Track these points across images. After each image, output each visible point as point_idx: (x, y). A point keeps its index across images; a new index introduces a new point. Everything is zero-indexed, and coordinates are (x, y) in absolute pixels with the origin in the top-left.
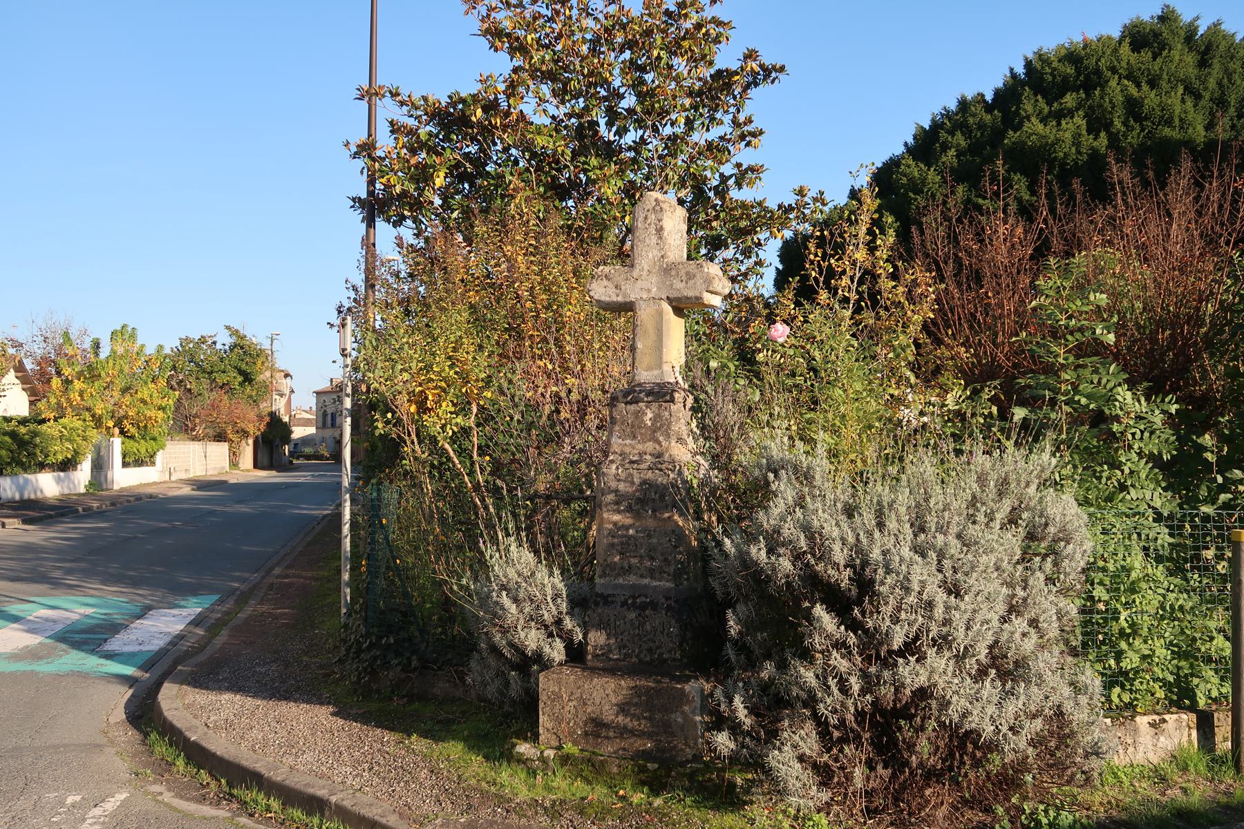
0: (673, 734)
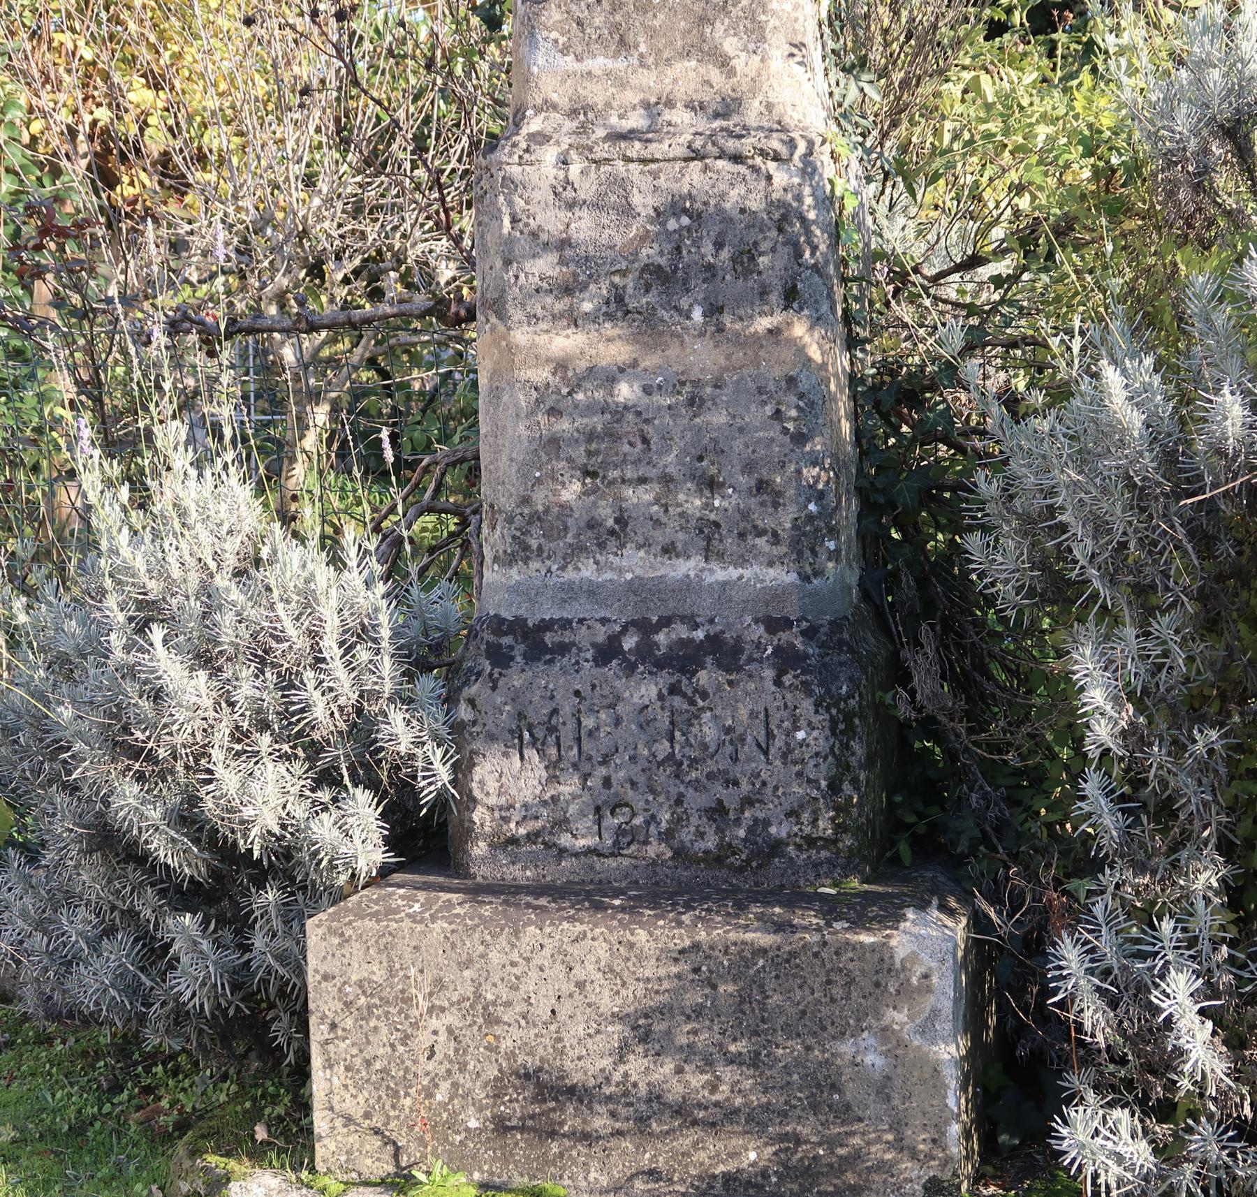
0: (845, 1113)
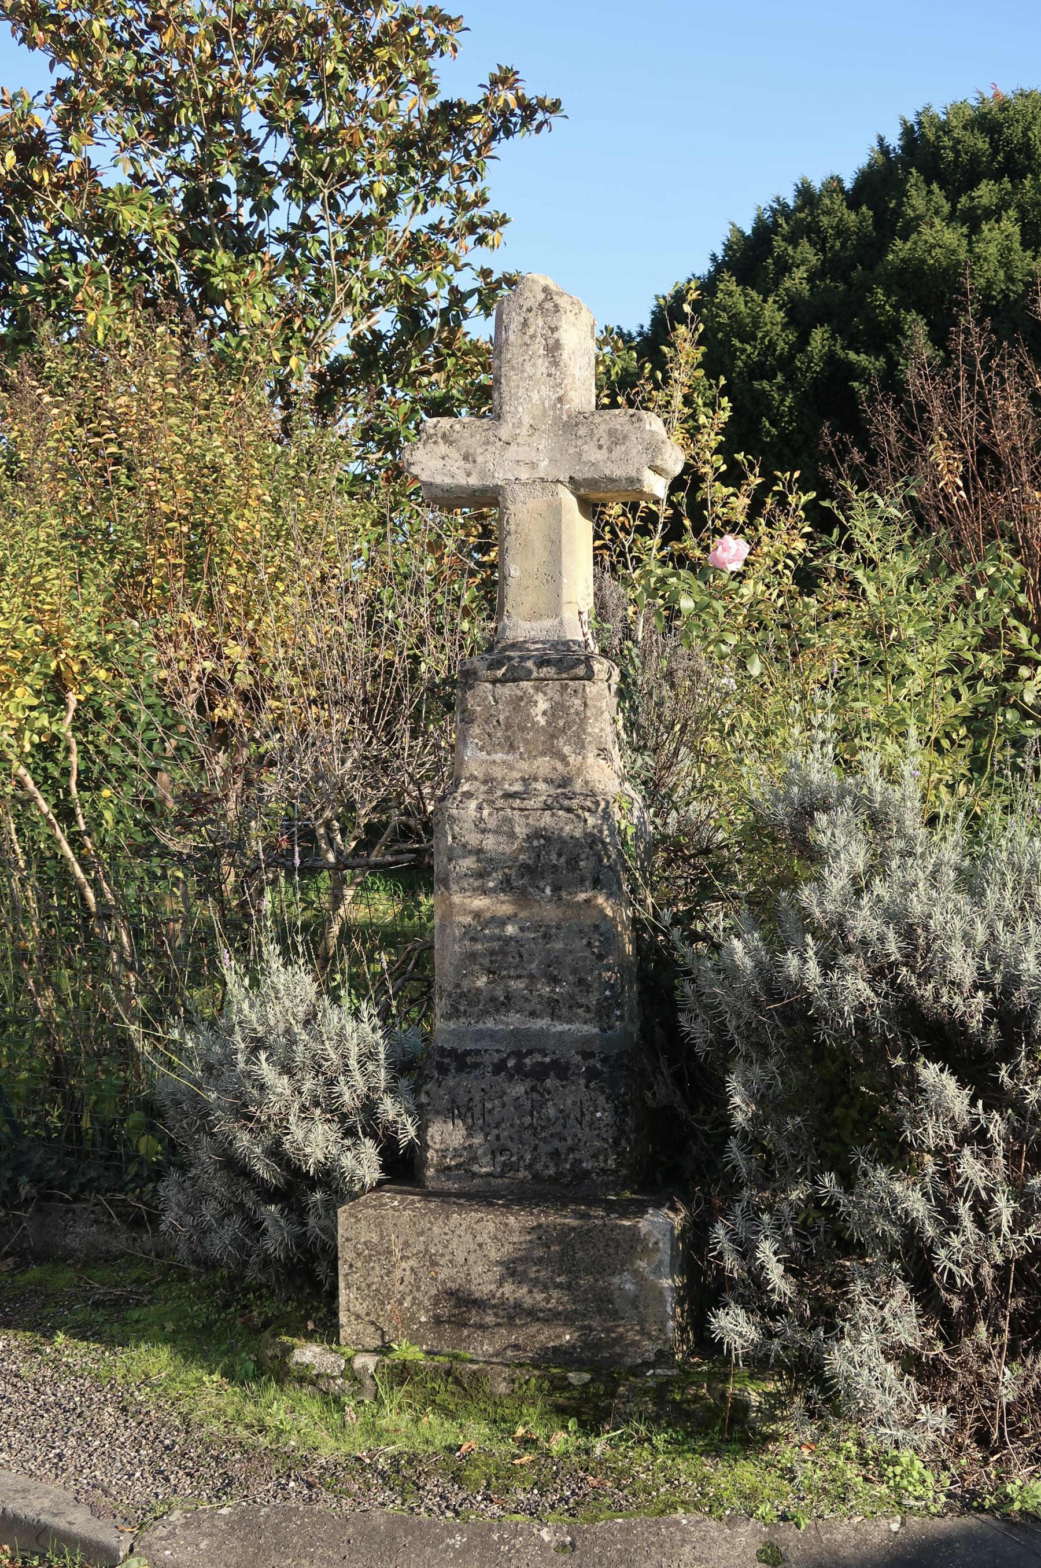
0: (615, 1315)
